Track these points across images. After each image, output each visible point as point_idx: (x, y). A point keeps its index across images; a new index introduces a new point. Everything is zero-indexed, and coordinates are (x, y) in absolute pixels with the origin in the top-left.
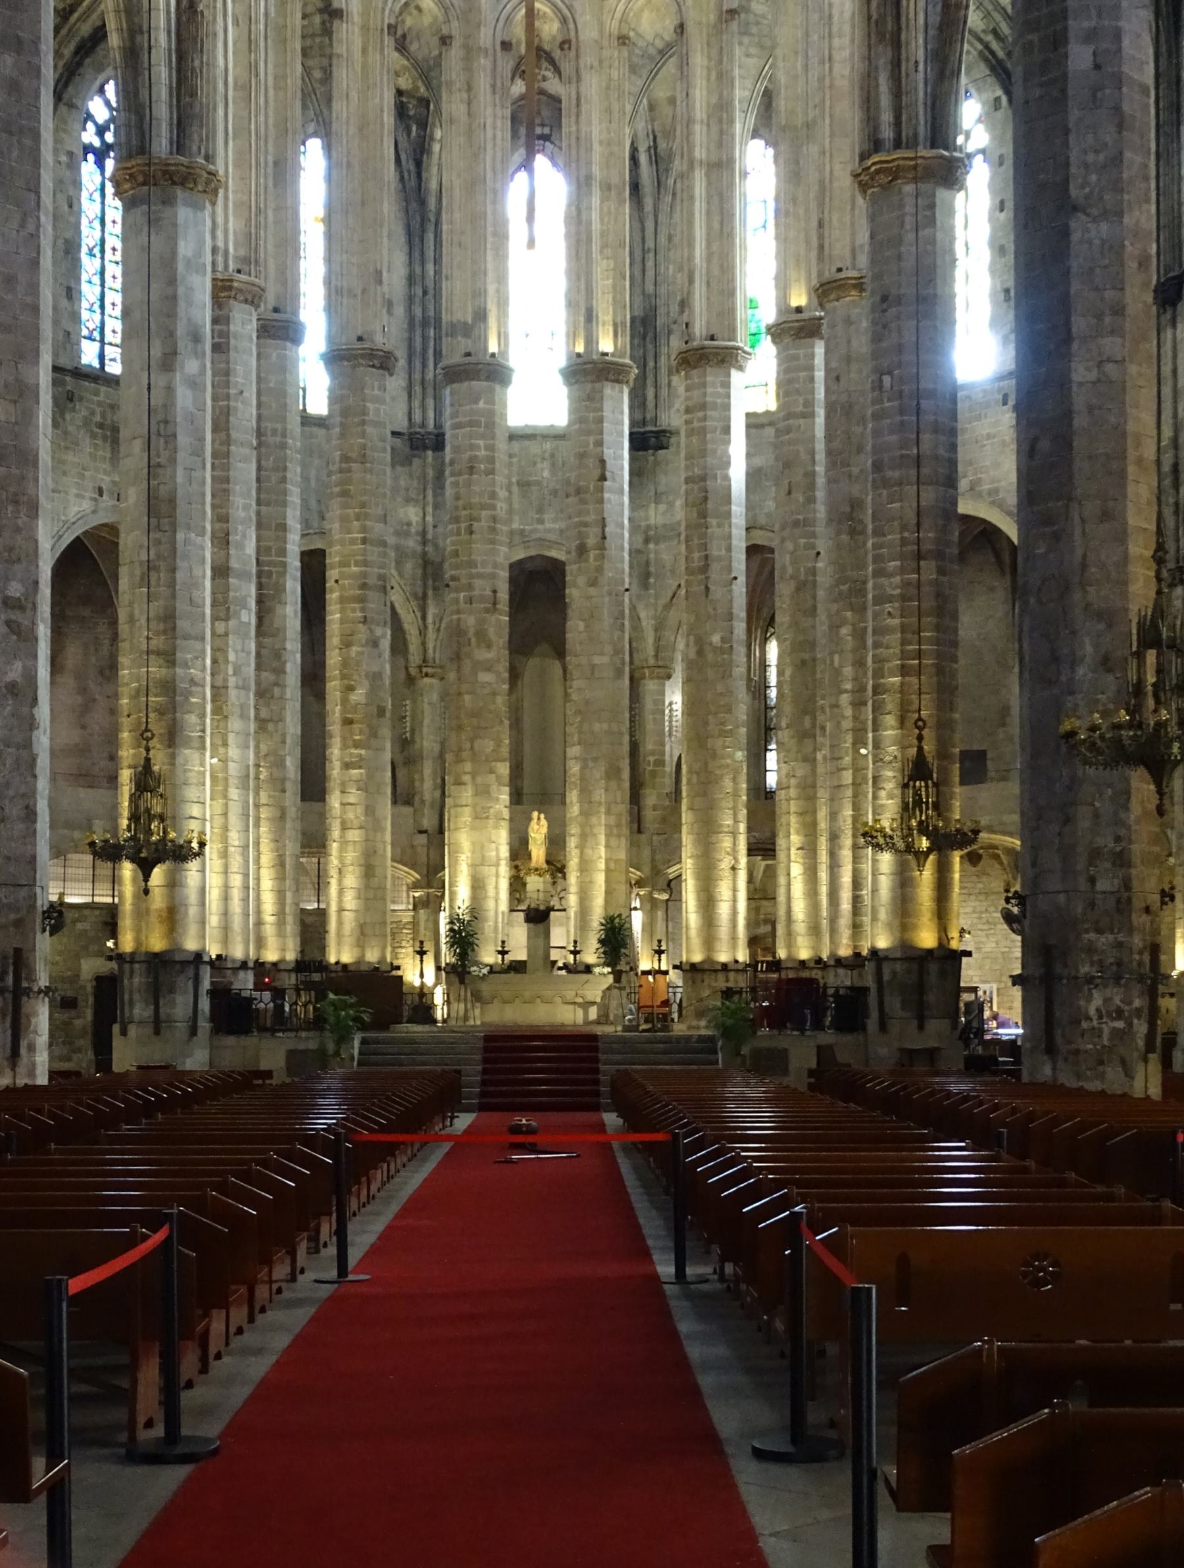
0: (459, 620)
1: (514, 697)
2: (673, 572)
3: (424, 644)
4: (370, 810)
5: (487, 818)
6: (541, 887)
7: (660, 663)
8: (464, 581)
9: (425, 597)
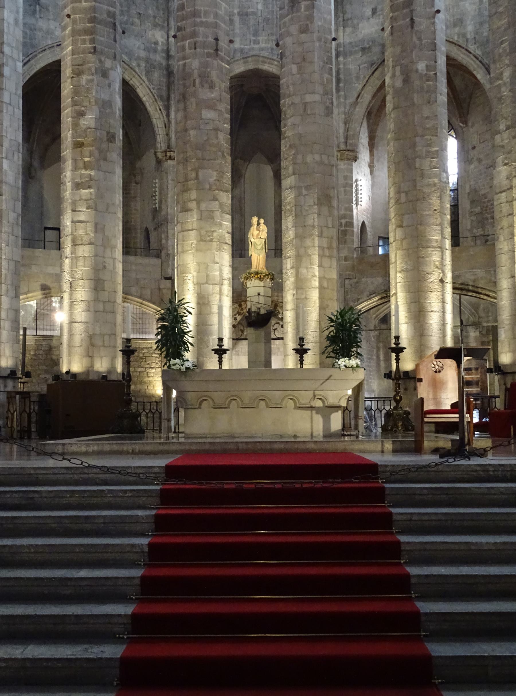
0: (184, 65)
1: (237, 191)
2: (358, 78)
3: (168, 134)
4: (98, 228)
5: (211, 240)
6: (262, 291)
7: (348, 148)
8: (189, 30)
9: (169, 98)
